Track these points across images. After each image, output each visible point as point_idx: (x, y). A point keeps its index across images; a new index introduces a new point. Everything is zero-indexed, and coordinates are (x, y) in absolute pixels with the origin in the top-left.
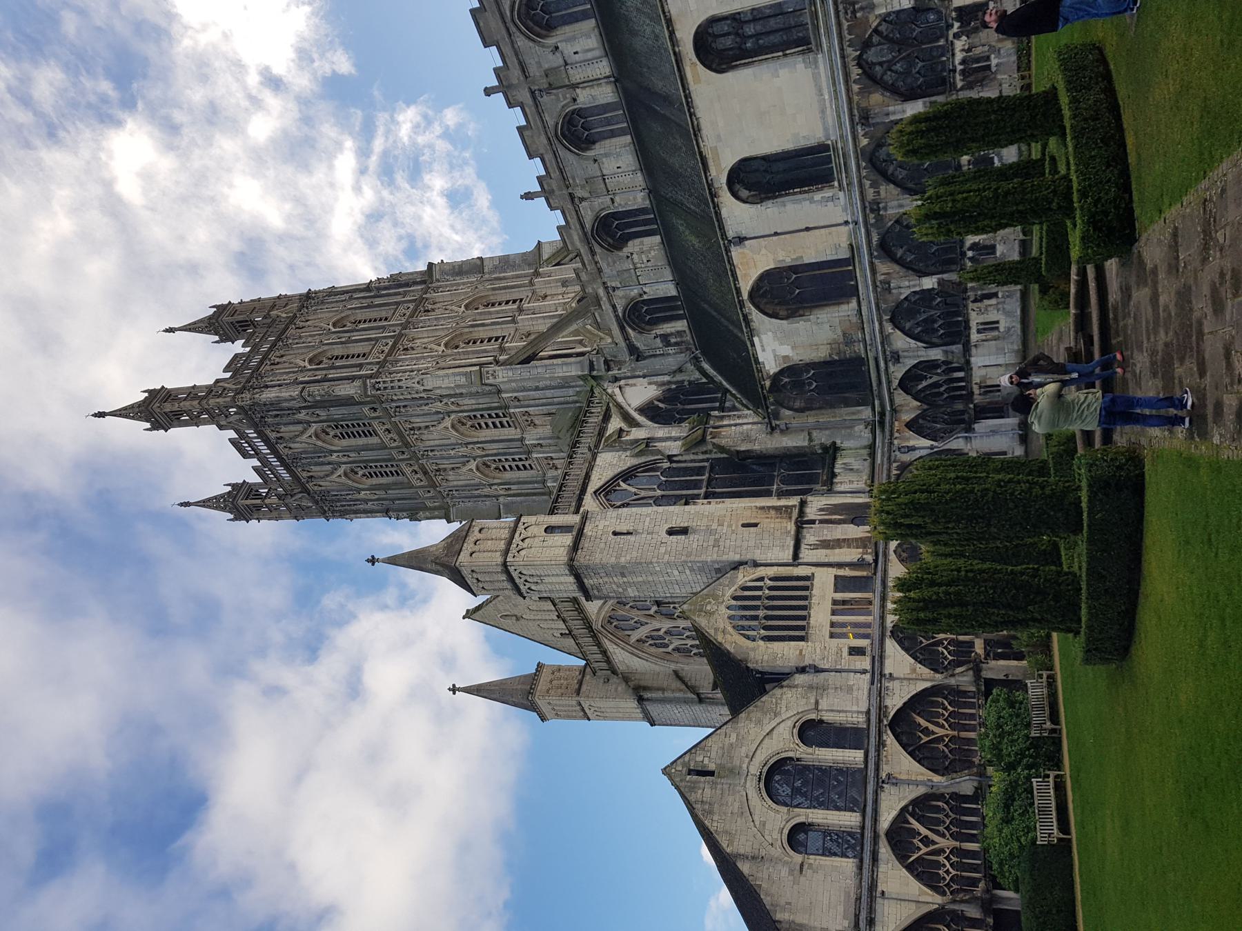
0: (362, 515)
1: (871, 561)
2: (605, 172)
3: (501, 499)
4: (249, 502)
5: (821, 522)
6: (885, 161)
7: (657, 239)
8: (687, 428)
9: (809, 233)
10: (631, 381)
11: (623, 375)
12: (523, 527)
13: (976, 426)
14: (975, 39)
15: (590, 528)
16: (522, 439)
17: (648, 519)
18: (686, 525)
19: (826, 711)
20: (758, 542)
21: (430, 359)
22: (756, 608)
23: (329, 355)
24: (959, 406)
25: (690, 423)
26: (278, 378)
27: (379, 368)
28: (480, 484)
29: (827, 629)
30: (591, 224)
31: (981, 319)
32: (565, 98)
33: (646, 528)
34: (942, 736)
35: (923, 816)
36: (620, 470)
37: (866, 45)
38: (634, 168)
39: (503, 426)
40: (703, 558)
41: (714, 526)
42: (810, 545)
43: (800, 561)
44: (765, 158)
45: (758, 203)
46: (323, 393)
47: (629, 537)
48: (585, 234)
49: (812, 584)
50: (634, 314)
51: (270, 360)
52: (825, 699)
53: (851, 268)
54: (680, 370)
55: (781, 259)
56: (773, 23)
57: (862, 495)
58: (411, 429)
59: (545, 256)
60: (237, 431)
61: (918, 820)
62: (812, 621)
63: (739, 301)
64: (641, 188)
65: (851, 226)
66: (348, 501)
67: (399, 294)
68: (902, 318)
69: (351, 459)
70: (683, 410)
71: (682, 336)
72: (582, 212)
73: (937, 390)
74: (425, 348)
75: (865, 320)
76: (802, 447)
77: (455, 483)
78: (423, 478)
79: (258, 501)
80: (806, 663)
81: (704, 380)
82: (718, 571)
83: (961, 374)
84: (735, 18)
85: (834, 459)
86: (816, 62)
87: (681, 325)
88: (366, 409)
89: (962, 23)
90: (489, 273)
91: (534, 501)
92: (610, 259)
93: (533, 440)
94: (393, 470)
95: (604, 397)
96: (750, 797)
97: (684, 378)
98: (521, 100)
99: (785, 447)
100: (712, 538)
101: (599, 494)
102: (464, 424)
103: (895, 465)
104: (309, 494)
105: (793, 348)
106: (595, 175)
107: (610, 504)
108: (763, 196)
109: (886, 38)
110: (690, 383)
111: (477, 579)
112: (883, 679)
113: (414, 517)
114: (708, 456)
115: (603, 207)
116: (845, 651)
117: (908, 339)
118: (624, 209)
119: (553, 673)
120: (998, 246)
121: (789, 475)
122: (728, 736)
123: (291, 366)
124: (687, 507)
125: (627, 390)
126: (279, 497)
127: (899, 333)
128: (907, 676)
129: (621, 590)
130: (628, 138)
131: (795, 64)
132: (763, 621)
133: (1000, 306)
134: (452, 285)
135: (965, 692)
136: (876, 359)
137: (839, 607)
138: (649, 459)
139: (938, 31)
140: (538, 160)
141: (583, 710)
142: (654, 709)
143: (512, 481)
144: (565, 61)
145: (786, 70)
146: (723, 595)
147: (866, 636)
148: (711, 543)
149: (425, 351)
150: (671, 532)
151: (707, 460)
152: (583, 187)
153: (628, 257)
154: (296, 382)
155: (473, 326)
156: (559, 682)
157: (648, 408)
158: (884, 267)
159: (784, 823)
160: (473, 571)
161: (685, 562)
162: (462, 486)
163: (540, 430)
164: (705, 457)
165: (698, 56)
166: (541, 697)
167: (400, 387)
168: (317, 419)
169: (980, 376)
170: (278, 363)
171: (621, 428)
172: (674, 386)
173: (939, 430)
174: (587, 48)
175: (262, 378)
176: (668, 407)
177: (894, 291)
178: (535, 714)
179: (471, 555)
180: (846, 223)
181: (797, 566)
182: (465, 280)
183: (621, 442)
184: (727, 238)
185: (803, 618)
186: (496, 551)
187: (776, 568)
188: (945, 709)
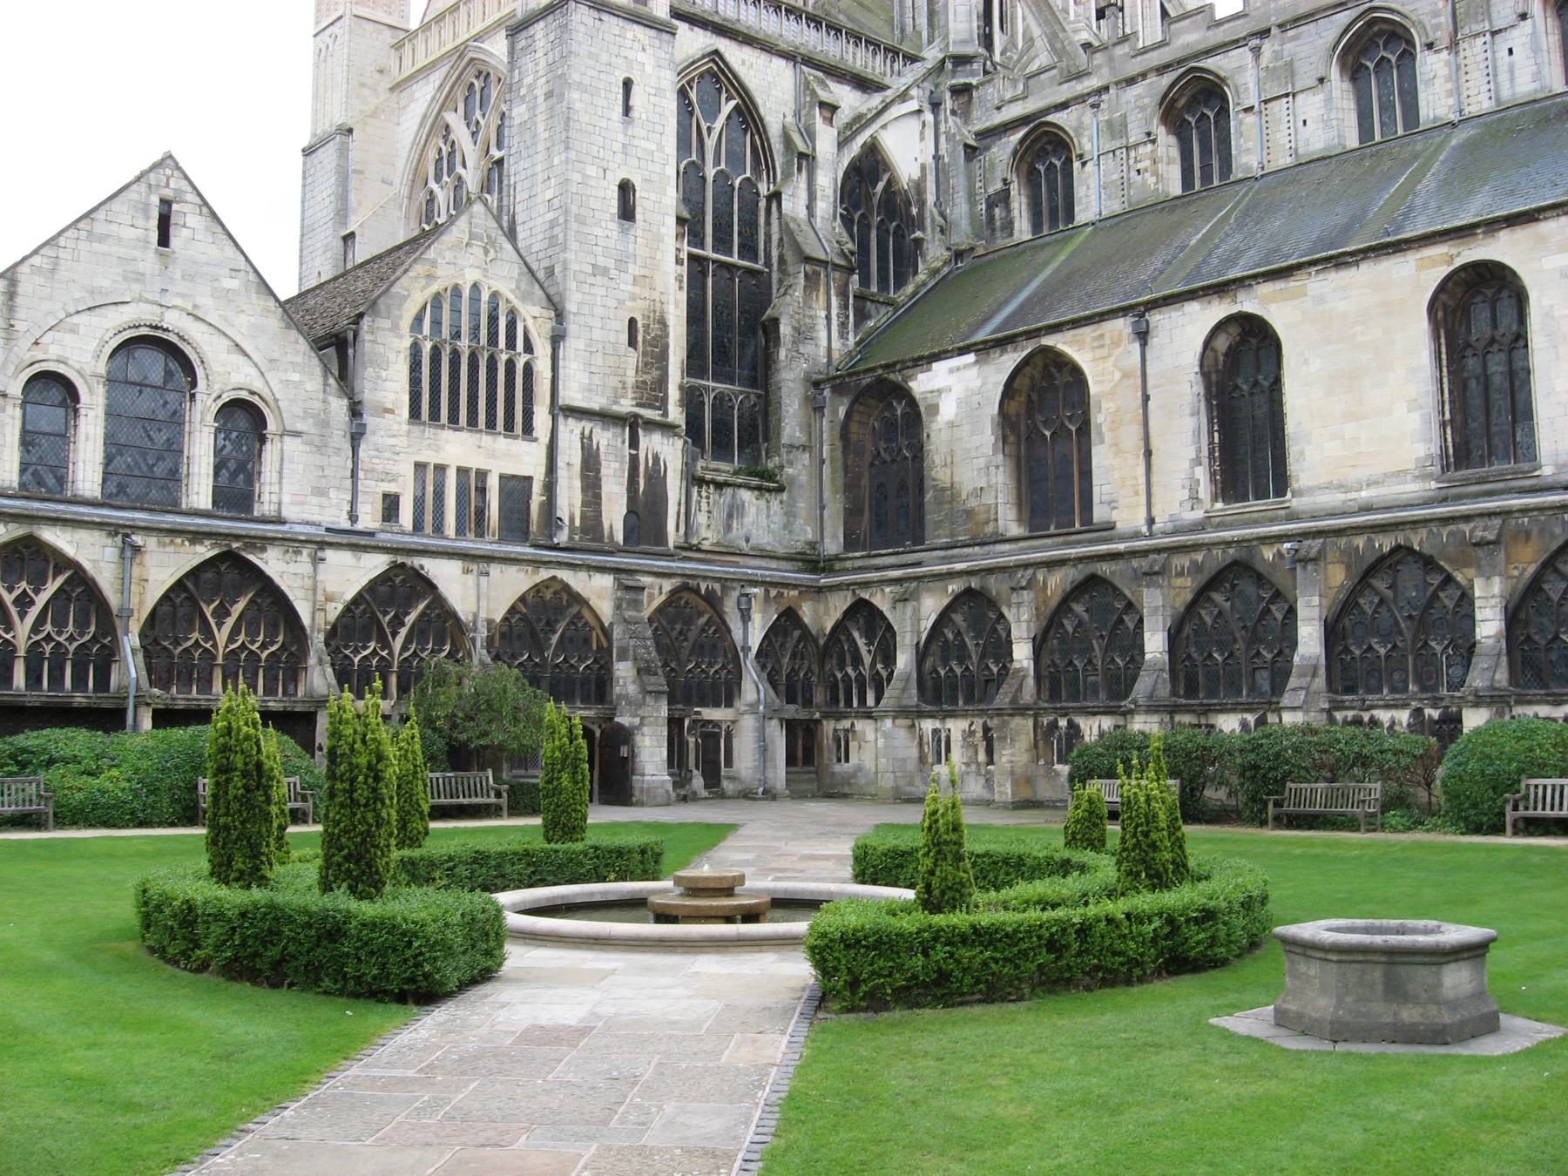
2: (1300, 97)
5: (634, 461)
6: (1233, 586)
7: (1176, 189)
9: (1141, 456)
11: (942, 117)
13: (775, 723)
15: (641, 37)
17: (653, 147)
18: (638, 216)
19: (282, 450)
24: (819, 696)
29: (432, 458)
30: (1211, 67)
31: (956, 736)
32: (1437, 27)
33: (636, 142)
34: (213, 638)
35: (69, 599)
36: (759, 101)
37: (1428, 563)
38: (1301, 151)
40: (573, 245)
41: (634, 269)
42: (590, 438)
43: (561, 419)
44: (1277, 381)
45: (1201, 366)
47: (620, 109)
48: (1197, 56)
49: (516, 437)
50: (1049, 143)
52: (302, 448)
53: (1077, 526)
55: (1104, 405)
56: (1500, 401)
57: (682, 529)
61: (60, 589)
62: (448, 434)
63: (1039, 330)
64: (1265, 162)
65: (1144, 529)
68: (971, 608)
70: (869, 226)
71: (1002, 229)
75: (987, 548)
80: (368, 419)
82: (550, 271)
83: (870, 700)
84: (1520, 339)
86: (1425, 477)
87: (1023, 229)
89: (1436, 722)
92: (1147, 100)
96: (121, 308)
97: (929, 230)
100: (611, 264)
101: (713, 61)
105: (952, 425)
106: (1297, 78)
107: (693, 79)
108: (1214, 377)
109: (1435, 596)
110: (918, 242)
112: (314, 546)
114: (775, 267)
115: (1241, 90)
116: (392, 488)
117: (933, 617)
118: (1232, 131)
122: (234, 273)
124: (671, 222)
125: (914, 124)
127: (946, 601)
128: (320, 587)
129: (523, 91)
132: (448, 349)
133: (973, 767)
135: (296, 681)
136: (918, 564)
137: (472, 482)
139: (1432, 682)
142: (328, 155)
144: (1500, 31)
147: (418, 526)
148: (601, 261)
150: (626, 189)
151: (768, 264)
152: (1277, 56)
157: (877, 162)
158: (1057, 582)
159: (77, 366)
161: (567, 212)
164: (775, 260)
165: (1464, 268)
169: (864, 732)
172: (914, 211)
173: (778, 661)
174: (1517, 73)
176: (875, 201)
177: (1014, 598)
180: (1151, 521)
183: (812, 108)
184: (1148, 310)
185: (454, 419)
187: (548, 374)
188: (264, 646)
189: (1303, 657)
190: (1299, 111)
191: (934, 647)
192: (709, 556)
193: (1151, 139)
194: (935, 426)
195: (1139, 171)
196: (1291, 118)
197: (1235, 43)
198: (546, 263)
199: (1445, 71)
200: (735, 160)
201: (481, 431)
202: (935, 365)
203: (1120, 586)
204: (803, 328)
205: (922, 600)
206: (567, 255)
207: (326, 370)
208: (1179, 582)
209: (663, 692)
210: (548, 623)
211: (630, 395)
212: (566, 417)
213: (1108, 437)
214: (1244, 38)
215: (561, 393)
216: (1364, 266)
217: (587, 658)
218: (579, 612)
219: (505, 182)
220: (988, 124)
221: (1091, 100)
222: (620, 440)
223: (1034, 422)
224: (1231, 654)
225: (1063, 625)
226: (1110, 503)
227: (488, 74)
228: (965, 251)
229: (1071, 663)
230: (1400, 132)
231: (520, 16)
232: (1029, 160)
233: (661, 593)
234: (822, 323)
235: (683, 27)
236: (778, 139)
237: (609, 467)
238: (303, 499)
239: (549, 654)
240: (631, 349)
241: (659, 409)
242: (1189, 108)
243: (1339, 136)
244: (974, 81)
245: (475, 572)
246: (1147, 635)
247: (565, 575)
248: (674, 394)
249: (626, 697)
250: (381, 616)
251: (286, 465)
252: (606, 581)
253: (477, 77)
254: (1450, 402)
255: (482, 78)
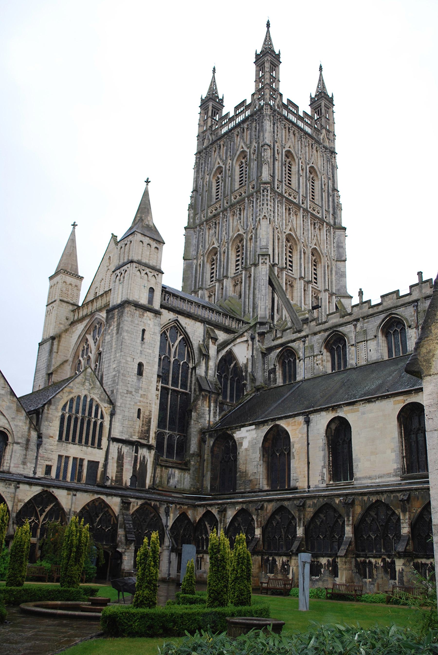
0: (196, 175)
1: (106, 484)
2: (369, 342)
3: (195, 261)
4: (210, 108)
5: (136, 457)
6: (327, 512)
7: (329, 371)
8: (213, 380)
9: (306, 464)
10: (250, 348)
11: (255, 343)
12: (155, 274)
14: (381, 571)
15: (149, 315)
16: (227, 277)
17: (151, 351)
18: (144, 374)
20: (127, 418)
21: (281, 224)
22: (84, 412)
23: (292, 163)
25: (216, 382)
26: (279, 131)
27: (278, 192)
28: (204, 248)
29: (64, 453)
32: (411, 321)
33: (145, 350)
37: (387, 506)
38: (369, 360)
39: (237, 265)
40: (121, 383)
41: (141, 392)
42: (121, 449)
43: (111, 442)
45: (326, 434)
46: (265, 158)
47: (141, 339)
48: (336, 326)
49: (95, 448)
50: (290, 353)
51: (292, 127)
52: (20, 448)
54: (254, 380)
58: (240, 209)
59: (343, 300)
60: (250, 104)
62: (71, 445)
63: (275, 418)
65: (307, 490)
66: (204, 167)
67: (329, 208)
69: (227, 171)
70: (227, 379)
72: (348, 326)
73: (204, 532)
74: (289, 221)
75: (256, 494)
76: (190, 450)
77: (207, 234)
78: (211, 215)
79: (210, 114)
80: (44, 440)
81: (245, 393)
82: (112, 392)
85: (179, 469)
86: (396, 476)
87: (280, 381)
88: (254, 183)
89: (390, 563)
90: (336, 265)
91: (192, 282)
93: (226, 284)
94: (219, 196)
95: (242, 330)
97: (248, 381)
98: (413, 293)
99: (190, 439)
100: (133, 390)
102: (240, 242)
103: (158, 503)
104: (211, 144)
105: (246, 450)
106: (368, 335)
107: (168, 329)
108: (330, 438)
110: (245, 385)
111: (126, 244)
112: (16, 483)
113: (191, 207)
114: (193, 392)
116: (49, 463)
117: (231, 518)
119: (76, 286)
120: (273, 575)
121: (175, 440)
122: (3, 389)
123: (287, 139)
124: (156, 376)
125: (245, 345)
126: (211, 127)
127: (235, 513)
128: (16, 497)
129: (110, 331)
130: (386, 358)
131: (397, 463)
132: (74, 416)
134: (330, 241)
138: (195, 355)
140: (379, 301)
141: (52, 303)
143: (205, 269)
145: (394, 457)
146: (94, 394)
148: (130, 389)
149: (287, 221)
150: (140, 365)
151: (190, 391)
152: (362, 328)
153: (321, 352)
154: (275, 142)
155: (300, 252)
156: (70, 289)
158: (270, 507)
160: (131, 242)
161: (119, 372)
162: (205, 238)
163: (232, 288)
164: (193, 390)
166: (61, 277)
167: (263, 204)
168: (251, 153)
169: (206, 558)
170: (289, 132)
171: (217, 339)
172: (244, 374)
175: (280, 122)
178: (53, 273)
179: (141, 241)
180: (309, 487)
181: (108, 440)
182: (332, 249)
183: (209, 339)
184: (310, 414)
186: (142, 257)
189: (346, 537)
190: (368, 346)
191: (231, 529)
192: (161, 492)
193: (321, 353)
194: (241, 450)
195: (317, 364)
196: (365, 349)
197: (348, 323)
198: (111, 389)
199: (415, 335)
200: (181, 355)
201: (83, 445)
202: (242, 429)
203: (290, 510)
204: (200, 414)
205: (228, 512)
206: (118, 387)
207: (31, 423)
208: (308, 509)
209: (134, 541)
210: (96, 514)
211: (137, 435)
212: (113, 442)
213: (296, 457)
214: (351, 321)
215: (112, 433)
216: (377, 402)
217: (109, 527)
218: (108, 510)
219: (101, 361)
220: (270, 346)
221: (303, 339)
222: (131, 450)
223: (274, 450)
224: (325, 536)
225: (272, 523)
226: (296, 480)
227: (101, 323)
228: (260, 388)
229: (275, 537)
230: (401, 355)
231: (111, 306)
232: (283, 358)
233: (137, 505)
234: (207, 412)
235: (164, 311)
236: (197, 349)
237: (127, 459)
238: (18, 465)
239: (95, 524)
240: (138, 419)
241: (146, 440)
242: (334, 343)
243: (381, 355)
244: (265, 331)
245: (72, 495)
246: (298, 528)
247: (103, 497)
248: (152, 435)
249: (120, 541)
250: (37, 508)
251: (13, 453)
252: (117, 500)
253: (98, 324)
254: (405, 450)
255: (99, 324)
